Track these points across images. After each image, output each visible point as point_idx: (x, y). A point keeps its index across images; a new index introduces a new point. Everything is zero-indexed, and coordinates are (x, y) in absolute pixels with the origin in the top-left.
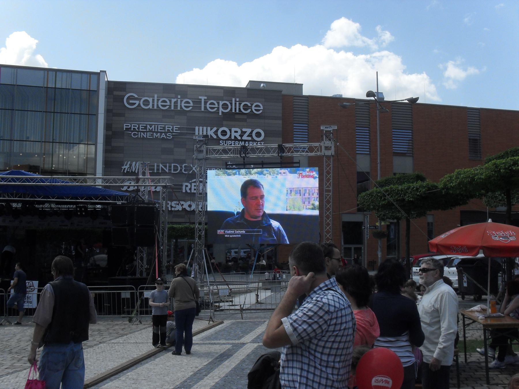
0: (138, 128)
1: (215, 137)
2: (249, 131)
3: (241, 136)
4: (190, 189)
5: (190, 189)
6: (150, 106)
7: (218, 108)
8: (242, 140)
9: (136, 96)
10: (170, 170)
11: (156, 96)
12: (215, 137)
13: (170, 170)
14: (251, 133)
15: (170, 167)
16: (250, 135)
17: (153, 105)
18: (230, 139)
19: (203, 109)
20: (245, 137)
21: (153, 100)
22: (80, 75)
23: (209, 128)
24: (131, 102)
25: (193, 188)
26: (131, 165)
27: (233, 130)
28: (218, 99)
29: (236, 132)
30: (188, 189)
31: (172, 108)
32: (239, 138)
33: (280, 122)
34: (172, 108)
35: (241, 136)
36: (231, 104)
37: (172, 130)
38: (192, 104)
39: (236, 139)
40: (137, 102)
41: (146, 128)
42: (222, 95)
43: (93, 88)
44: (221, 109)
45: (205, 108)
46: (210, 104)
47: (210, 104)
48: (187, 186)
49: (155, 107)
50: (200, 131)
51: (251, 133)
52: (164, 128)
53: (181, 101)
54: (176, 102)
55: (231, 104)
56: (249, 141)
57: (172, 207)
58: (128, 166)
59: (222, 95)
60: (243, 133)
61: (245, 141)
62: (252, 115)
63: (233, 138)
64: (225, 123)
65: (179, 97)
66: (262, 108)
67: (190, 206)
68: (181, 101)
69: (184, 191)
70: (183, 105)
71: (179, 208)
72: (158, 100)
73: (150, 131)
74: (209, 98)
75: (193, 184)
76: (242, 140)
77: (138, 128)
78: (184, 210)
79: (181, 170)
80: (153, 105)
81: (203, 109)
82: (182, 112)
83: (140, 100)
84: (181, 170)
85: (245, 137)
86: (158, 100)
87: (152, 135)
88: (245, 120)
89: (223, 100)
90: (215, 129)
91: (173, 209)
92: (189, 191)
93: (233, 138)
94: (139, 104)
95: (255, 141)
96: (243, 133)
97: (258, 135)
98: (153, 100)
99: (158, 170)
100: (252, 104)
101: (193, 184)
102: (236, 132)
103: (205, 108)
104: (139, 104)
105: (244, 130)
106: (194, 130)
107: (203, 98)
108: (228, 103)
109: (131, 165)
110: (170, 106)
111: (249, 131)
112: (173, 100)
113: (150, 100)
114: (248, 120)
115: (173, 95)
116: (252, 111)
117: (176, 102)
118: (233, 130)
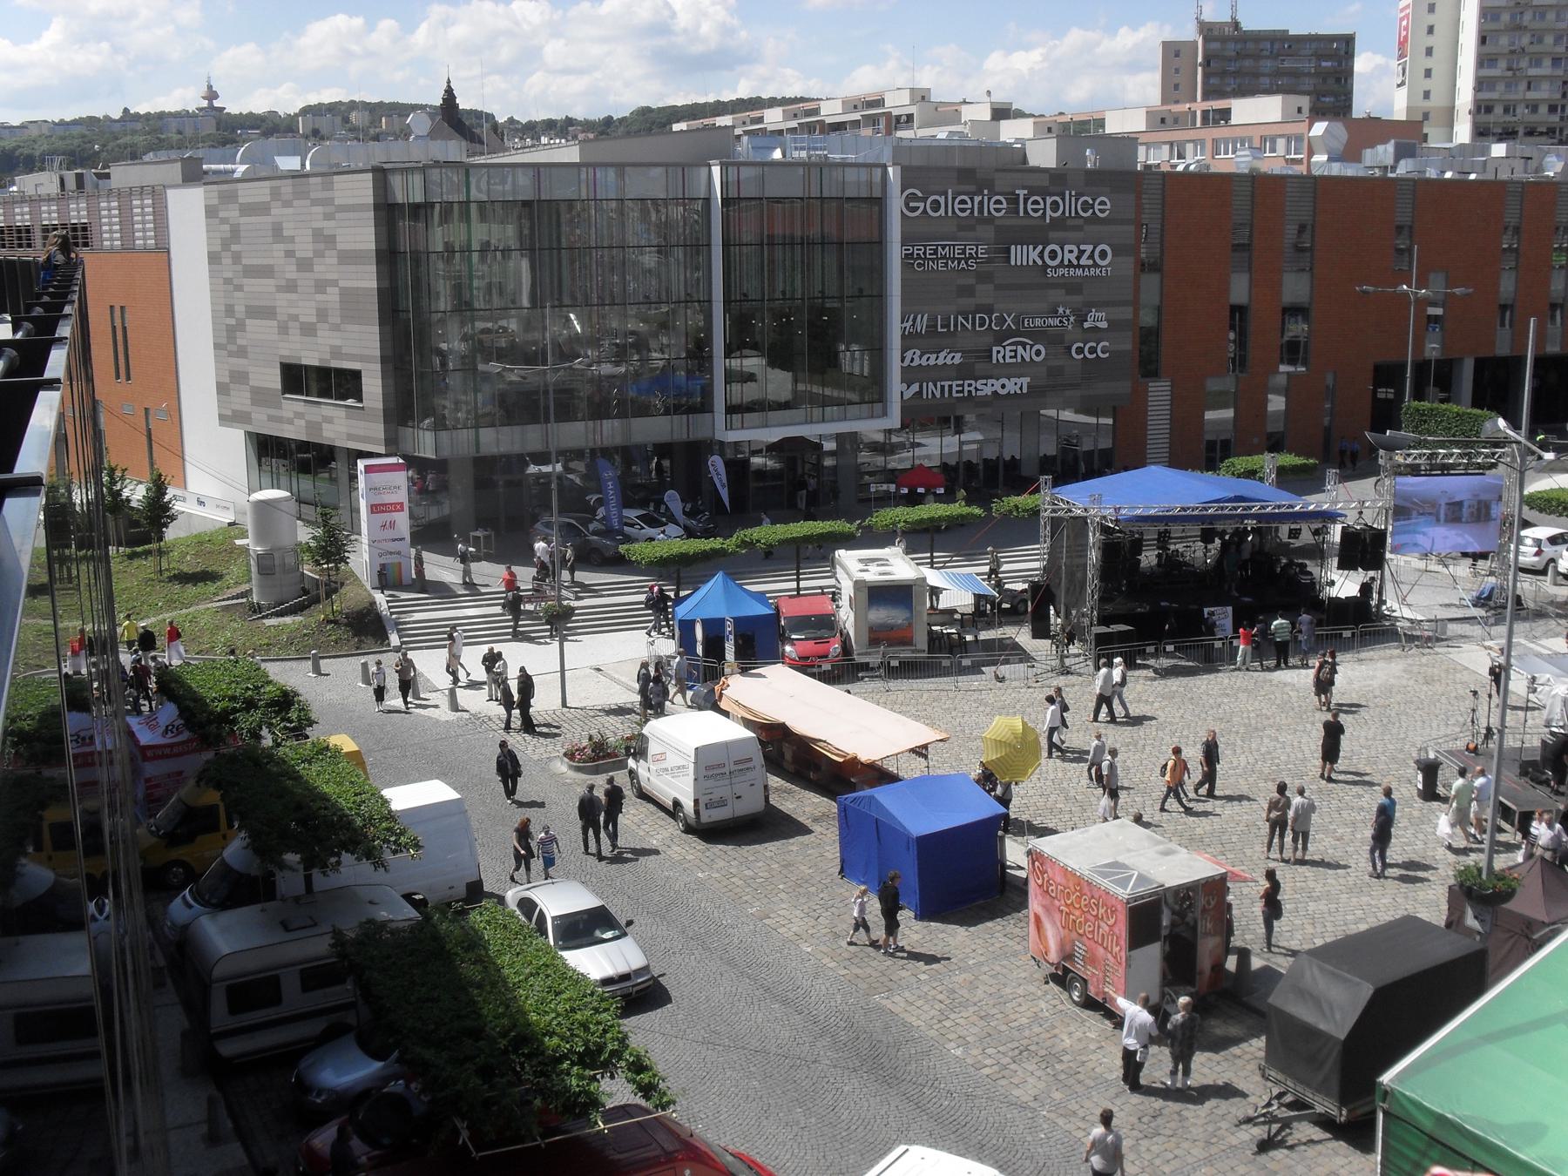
0: (925, 253)
1: (1040, 262)
2: (1089, 248)
3: (1078, 258)
4: (1004, 357)
5: (1004, 357)
6: (942, 212)
7: (1045, 209)
8: (1079, 266)
9: (920, 195)
10: (974, 324)
11: (950, 191)
12: (1040, 262)
13: (974, 324)
14: (1093, 252)
15: (974, 319)
16: (1091, 256)
17: (946, 212)
18: (1061, 265)
19: (1021, 214)
20: (1084, 261)
21: (946, 198)
22: (856, 169)
23: (1031, 247)
24: (911, 204)
25: (1008, 354)
26: (914, 320)
27: (1067, 247)
28: (1044, 193)
29: (1071, 252)
30: (1000, 356)
31: (976, 214)
32: (1075, 262)
33: (1132, 228)
34: (976, 214)
35: (1078, 258)
36: (1063, 200)
37: (976, 253)
38: (1005, 205)
39: (1071, 265)
40: (921, 205)
41: (936, 252)
42: (1046, 183)
43: (877, 193)
44: (1049, 212)
45: (1025, 208)
46: (1033, 203)
47: (1033, 203)
48: (998, 352)
49: (950, 214)
50: (1024, 255)
51: (1093, 252)
52: (964, 252)
53: (989, 199)
54: (981, 203)
55: (1063, 200)
56: (1089, 267)
57: (976, 389)
58: (910, 323)
59: (1046, 183)
60: (1082, 252)
61: (1083, 267)
62: (1094, 219)
63: (1066, 263)
64: (1052, 235)
65: (986, 192)
66: (1108, 206)
67: (1003, 386)
68: (989, 199)
69: (994, 361)
70: (992, 206)
71: (988, 391)
72: (954, 199)
73: (944, 257)
74: (1031, 194)
75: (1008, 348)
76: (1079, 266)
77: (925, 253)
78: (995, 393)
79: (990, 325)
80: (946, 212)
81: (1021, 214)
82: (991, 219)
83: (924, 200)
84: (990, 325)
85: (1084, 261)
86: (954, 199)
87: (946, 264)
88: (1078, 228)
89: (1051, 195)
90: (1040, 247)
91: (979, 393)
92: (1001, 361)
93: (1066, 263)
94: (925, 211)
95: (1099, 266)
96: (1082, 252)
97: (1103, 255)
98: (946, 198)
99: (956, 326)
100: (1094, 200)
101: (1008, 348)
102: (1071, 252)
103: (1025, 208)
104: (925, 211)
105: (1082, 247)
106: (1008, 251)
107: (1022, 193)
108: (1057, 198)
109: (914, 320)
110: (972, 209)
111: (1089, 248)
112: (977, 199)
113: (942, 200)
114: (1086, 227)
115: (972, 188)
116: (1094, 213)
117: (981, 203)
118: (1067, 247)
